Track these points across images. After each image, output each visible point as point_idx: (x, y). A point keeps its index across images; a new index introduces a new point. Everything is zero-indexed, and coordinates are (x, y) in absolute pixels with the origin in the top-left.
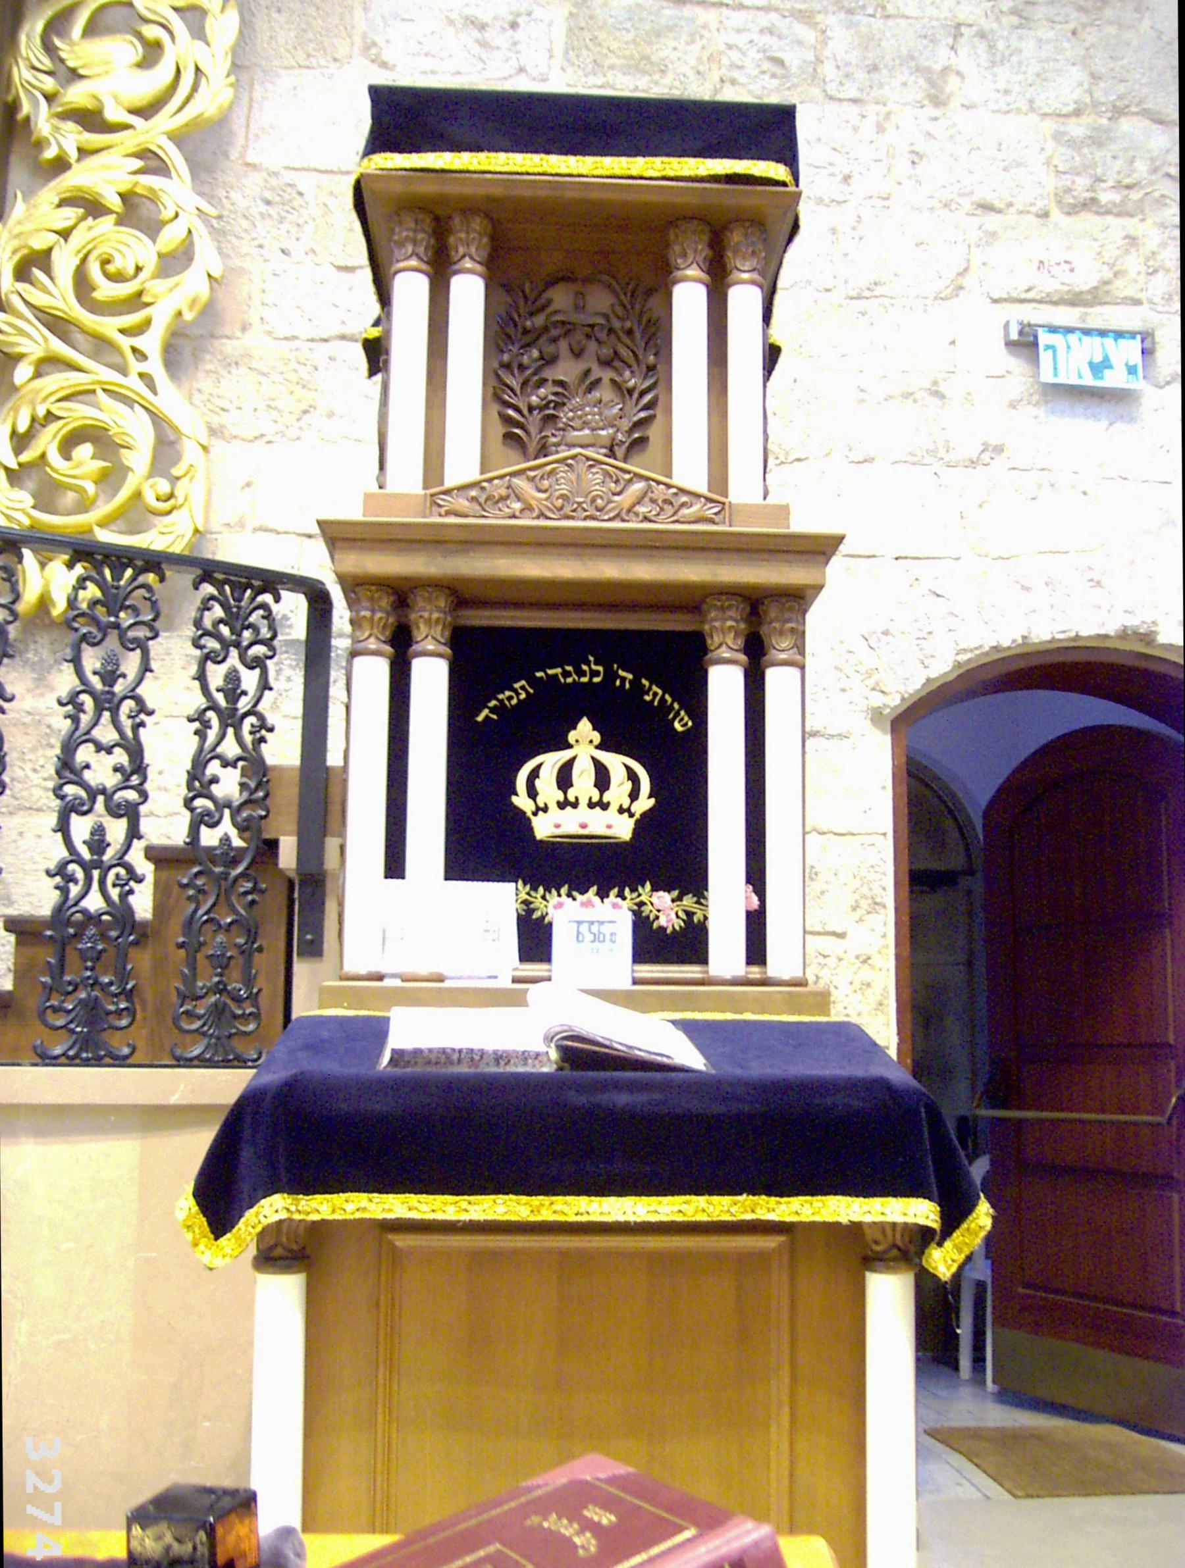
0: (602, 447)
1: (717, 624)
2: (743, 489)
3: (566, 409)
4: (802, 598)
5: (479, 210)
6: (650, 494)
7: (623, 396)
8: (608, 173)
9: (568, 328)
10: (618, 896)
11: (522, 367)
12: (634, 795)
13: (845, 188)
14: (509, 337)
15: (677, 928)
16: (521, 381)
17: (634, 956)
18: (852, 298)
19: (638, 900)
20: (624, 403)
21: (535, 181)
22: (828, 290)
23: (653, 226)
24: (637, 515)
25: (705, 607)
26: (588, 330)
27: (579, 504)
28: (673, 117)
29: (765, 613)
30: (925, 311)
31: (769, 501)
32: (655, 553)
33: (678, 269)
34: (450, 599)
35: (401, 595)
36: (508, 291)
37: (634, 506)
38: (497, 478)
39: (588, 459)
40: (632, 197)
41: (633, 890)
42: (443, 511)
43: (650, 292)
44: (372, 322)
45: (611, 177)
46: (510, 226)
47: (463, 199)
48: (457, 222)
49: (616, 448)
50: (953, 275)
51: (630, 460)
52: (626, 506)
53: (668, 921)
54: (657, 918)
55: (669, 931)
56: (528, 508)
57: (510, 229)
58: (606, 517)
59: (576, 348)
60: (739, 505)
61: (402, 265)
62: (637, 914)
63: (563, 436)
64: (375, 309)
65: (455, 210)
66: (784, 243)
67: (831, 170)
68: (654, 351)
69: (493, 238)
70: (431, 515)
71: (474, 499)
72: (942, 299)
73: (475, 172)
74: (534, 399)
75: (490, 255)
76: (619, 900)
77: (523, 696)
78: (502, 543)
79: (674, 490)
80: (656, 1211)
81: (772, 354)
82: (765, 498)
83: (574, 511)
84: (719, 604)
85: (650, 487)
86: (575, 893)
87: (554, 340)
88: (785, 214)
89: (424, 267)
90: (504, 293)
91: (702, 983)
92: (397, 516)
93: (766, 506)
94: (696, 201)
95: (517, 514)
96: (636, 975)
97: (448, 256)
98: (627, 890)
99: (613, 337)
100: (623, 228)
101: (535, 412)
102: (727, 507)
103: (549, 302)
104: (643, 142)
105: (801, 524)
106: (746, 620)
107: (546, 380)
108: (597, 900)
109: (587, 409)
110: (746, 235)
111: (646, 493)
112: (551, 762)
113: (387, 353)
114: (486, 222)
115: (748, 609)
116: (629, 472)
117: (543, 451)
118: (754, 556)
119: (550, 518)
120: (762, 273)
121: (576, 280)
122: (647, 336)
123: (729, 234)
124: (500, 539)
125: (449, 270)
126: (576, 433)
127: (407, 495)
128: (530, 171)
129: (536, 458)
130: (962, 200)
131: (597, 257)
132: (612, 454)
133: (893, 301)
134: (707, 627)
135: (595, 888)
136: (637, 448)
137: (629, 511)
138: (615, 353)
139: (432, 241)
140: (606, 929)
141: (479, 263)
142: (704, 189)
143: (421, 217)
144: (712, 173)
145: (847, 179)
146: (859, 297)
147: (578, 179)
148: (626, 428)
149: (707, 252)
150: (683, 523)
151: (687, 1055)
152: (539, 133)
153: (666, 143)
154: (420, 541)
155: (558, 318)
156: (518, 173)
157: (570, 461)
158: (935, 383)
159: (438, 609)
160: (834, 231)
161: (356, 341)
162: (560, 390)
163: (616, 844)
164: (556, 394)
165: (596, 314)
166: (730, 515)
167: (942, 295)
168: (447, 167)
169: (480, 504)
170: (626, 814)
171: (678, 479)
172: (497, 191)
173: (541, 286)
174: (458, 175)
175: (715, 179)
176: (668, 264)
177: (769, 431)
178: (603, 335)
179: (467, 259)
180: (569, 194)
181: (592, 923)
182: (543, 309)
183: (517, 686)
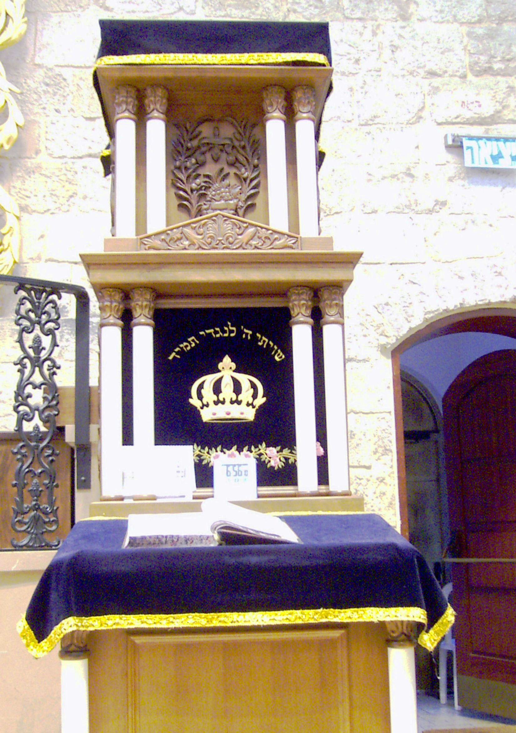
0: (231, 210)
1: (296, 303)
2: (308, 230)
3: (211, 190)
4: (341, 287)
5: (161, 85)
6: (257, 234)
7: (241, 182)
8: (229, 62)
9: (210, 146)
10: (248, 450)
11: (186, 168)
12: (255, 396)
13: (357, 66)
14: (179, 152)
15: (280, 467)
16: (186, 176)
17: (258, 483)
18: (362, 125)
19: (259, 452)
20: (242, 185)
21: (190, 68)
22: (349, 121)
23: (254, 90)
24: (251, 245)
25: (289, 294)
26: (221, 147)
27: (220, 241)
28: (263, 31)
29: (322, 296)
30: (402, 131)
31: (322, 235)
32: (261, 265)
33: (269, 113)
34: (152, 294)
35: (126, 293)
36: (178, 128)
37: (249, 241)
38: (175, 228)
39: (224, 216)
40: (242, 75)
41: (256, 447)
42: (147, 247)
43: (254, 126)
44: (105, 147)
45: (231, 65)
46: (177, 93)
47: (152, 79)
48: (149, 92)
49: (238, 210)
50: (416, 111)
51: (246, 216)
52: (245, 241)
53: (275, 463)
54: (269, 461)
55: (276, 468)
56: (193, 244)
57: (178, 95)
58: (235, 247)
59: (215, 157)
60: (305, 238)
61: (120, 116)
62: (259, 460)
63: (210, 205)
64: (106, 140)
65: (148, 85)
66: (325, 97)
67: (349, 56)
68: (257, 157)
69: (169, 100)
70: (141, 249)
71: (163, 240)
72: (411, 124)
73: (158, 65)
74: (194, 186)
75: (167, 109)
76: (249, 452)
77: (193, 345)
78: (179, 263)
79: (270, 232)
80: (274, 619)
81: (321, 157)
82: (319, 234)
83: (217, 244)
84: (297, 292)
85: (257, 230)
86: (225, 450)
87: (204, 153)
88: (325, 81)
89: (132, 116)
90: (176, 129)
91: (295, 496)
92: (122, 251)
93: (320, 238)
94: (276, 76)
95: (187, 247)
96: (259, 493)
97: (145, 110)
98: (253, 447)
99: (235, 150)
100: (239, 92)
101: (195, 192)
102: (299, 240)
103: (200, 133)
104: (247, 45)
105: (339, 247)
106: (312, 300)
107: (200, 175)
108: (237, 453)
109: (222, 190)
110: (304, 94)
111: (256, 233)
112: (209, 379)
113: (114, 163)
114: (165, 91)
115: (312, 294)
116: (246, 223)
117: (200, 212)
118: (314, 265)
119: (205, 249)
120: (314, 114)
121: (214, 120)
122: (253, 149)
123: (295, 93)
124: (178, 261)
125: (146, 118)
126: (217, 203)
127: (127, 239)
128: (188, 62)
129: (196, 217)
130: (419, 71)
131: (225, 108)
132: (236, 213)
133: (384, 126)
134: (291, 305)
135: (235, 447)
136: (249, 209)
137: (247, 244)
138: (236, 159)
139: (136, 102)
140: (242, 468)
141: (162, 113)
142: (281, 69)
143: (130, 89)
144: (285, 60)
145: (357, 61)
146: (366, 125)
147: (213, 66)
148: (244, 199)
149: (284, 103)
150: (276, 249)
151: (289, 535)
152: (191, 42)
153: (260, 45)
154: (135, 264)
155: (205, 141)
156: (181, 64)
157: (214, 218)
158: (409, 169)
159: (146, 300)
160: (351, 89)
161: (97, 157)
162: (207, 180)
163: (246, 423)
164: (205, 182)
165: (226, 138)
166: (301, 244)
167: (411, 122)
168: (143, 62)
169: (167, 243)
170: (251, 407)
171: (273, 225)
172: (170, 74)
173: (195, 125)
174: (149, 66)
175: (287, 64)
176: (263, 111)
177: (320, 198)
178: (229, 150)
179: (155, 111)
180: (209, 75)
181: (234, 466)
182: (197, 137)
183: (190, 339)
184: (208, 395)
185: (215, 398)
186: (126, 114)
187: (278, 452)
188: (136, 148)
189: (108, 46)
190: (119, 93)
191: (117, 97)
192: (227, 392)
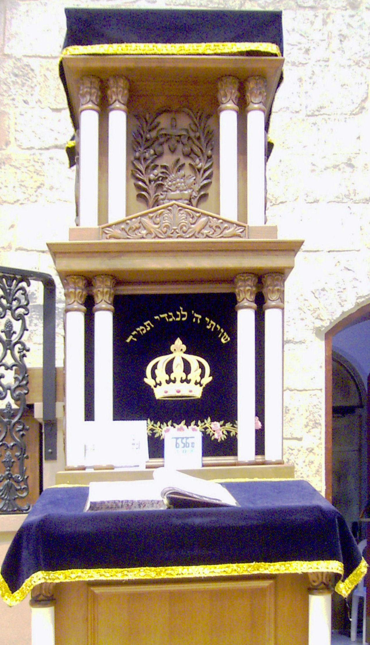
10: (195, 425)
12: (202, 376)
15: (223, 439)
17: (203, 453)
19: (204, 426)
41: (202, 422)
53: (218, 436)
54: (214, 434)
55: (219, 441)
62: (204, 433)
76: (196, 426)
77: (149, 329)
80: (213, 572)
86: (175, 424)
91: (234, 465)
96: (204, 462)
98: (199, 422)
108: (185, 427)
112: (162, 360)
135: (184, 422)
140: (190, 441)
151: (228, 499)
163: (194, 400)
170: (199, 385)
181: (183, 438)
183: (146, 324)
184: (161, 375)
185: (167, 377)
186: (90, 105)
187: (221, 426)
188: (99, 139)
189: (73, 36)
190: (83, 84)
191: (82, 88)
192: (178, 372)
